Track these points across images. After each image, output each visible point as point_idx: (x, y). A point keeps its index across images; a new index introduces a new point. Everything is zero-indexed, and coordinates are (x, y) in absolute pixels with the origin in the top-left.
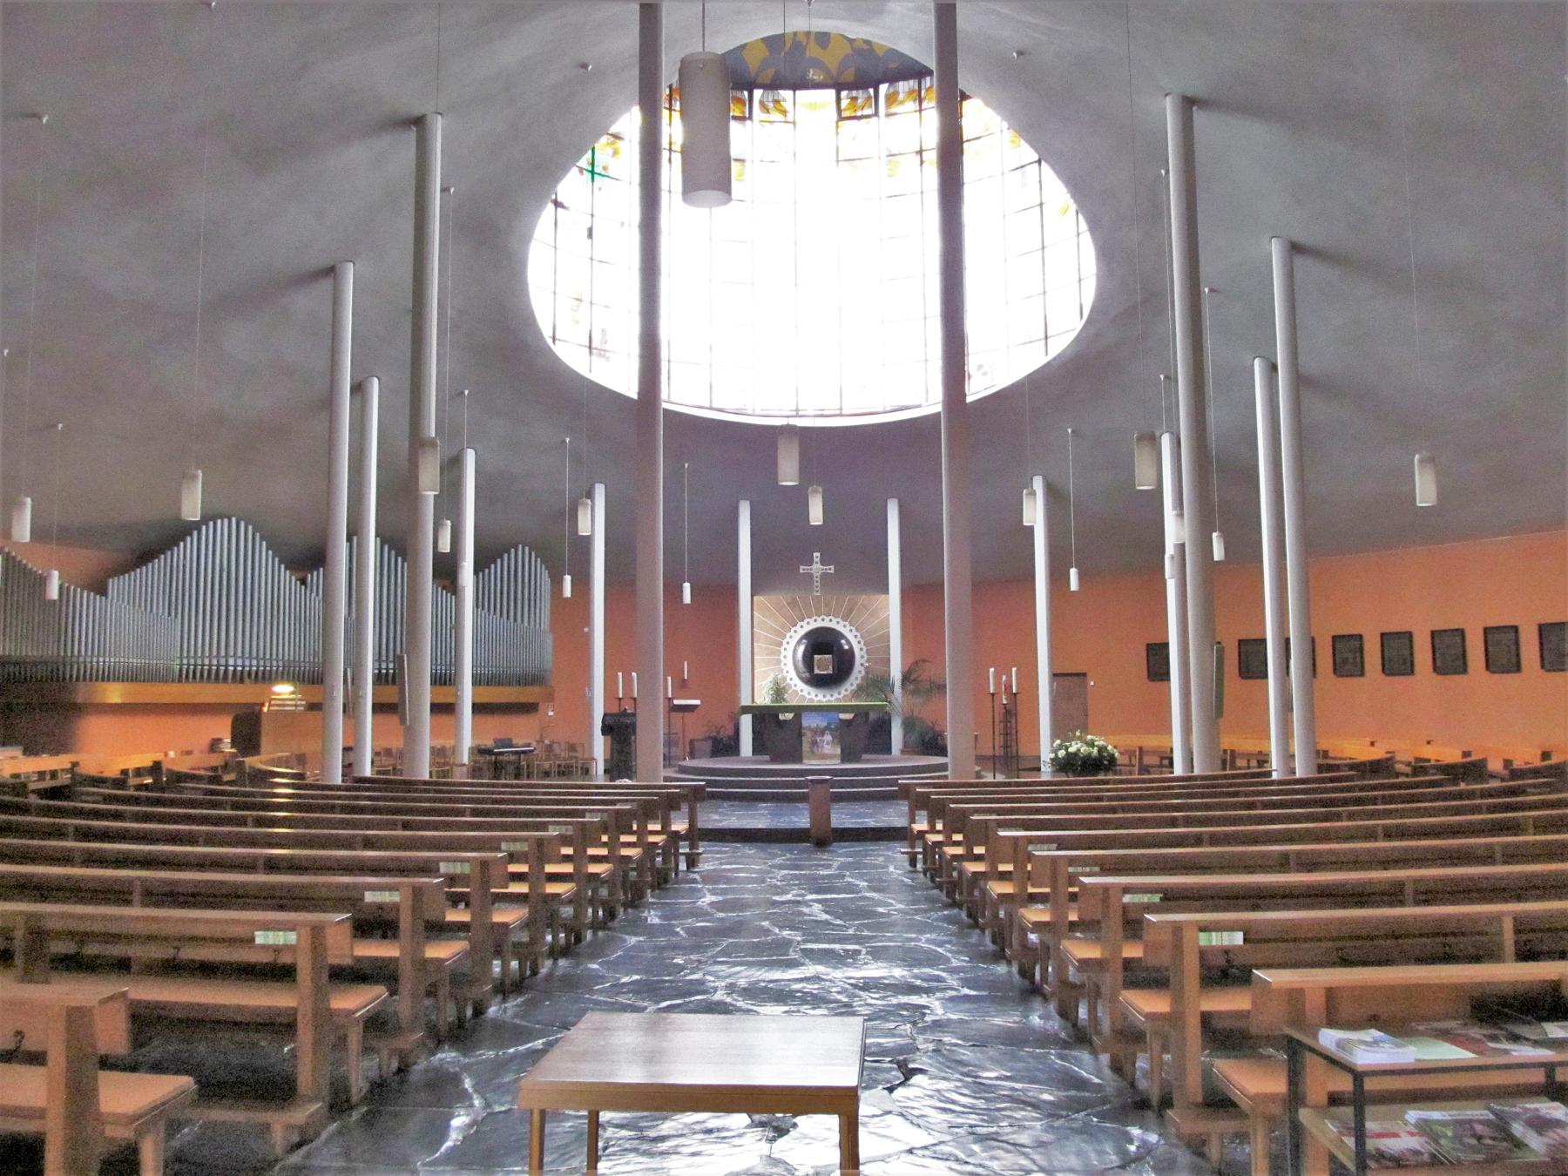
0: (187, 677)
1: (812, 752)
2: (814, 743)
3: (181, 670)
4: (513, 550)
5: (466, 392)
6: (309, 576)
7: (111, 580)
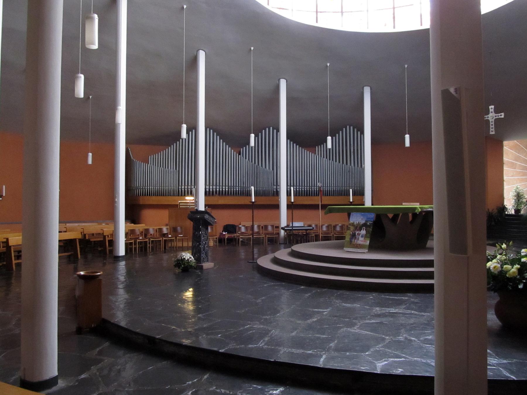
0: (236, 194)
1: (351, 241)
2: (353, 236)
3: (179, 191)
4: (344, 129)
5: (252, 48)
6: (242, 149)
7: (150, 157)
